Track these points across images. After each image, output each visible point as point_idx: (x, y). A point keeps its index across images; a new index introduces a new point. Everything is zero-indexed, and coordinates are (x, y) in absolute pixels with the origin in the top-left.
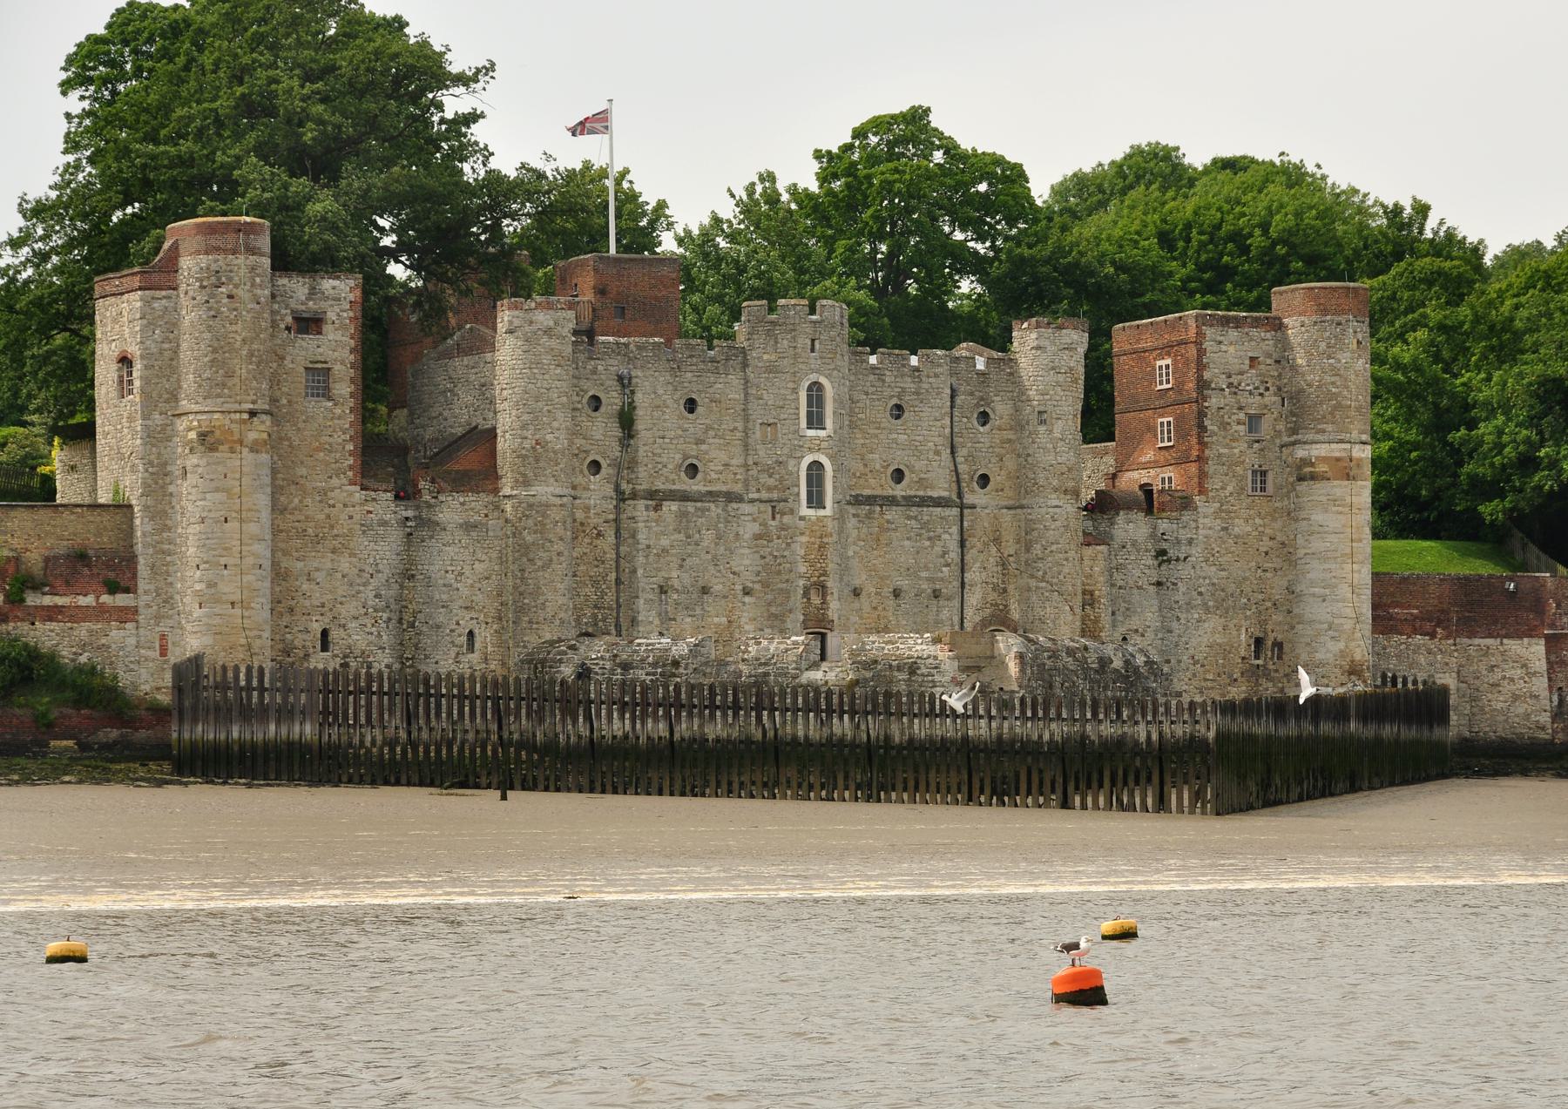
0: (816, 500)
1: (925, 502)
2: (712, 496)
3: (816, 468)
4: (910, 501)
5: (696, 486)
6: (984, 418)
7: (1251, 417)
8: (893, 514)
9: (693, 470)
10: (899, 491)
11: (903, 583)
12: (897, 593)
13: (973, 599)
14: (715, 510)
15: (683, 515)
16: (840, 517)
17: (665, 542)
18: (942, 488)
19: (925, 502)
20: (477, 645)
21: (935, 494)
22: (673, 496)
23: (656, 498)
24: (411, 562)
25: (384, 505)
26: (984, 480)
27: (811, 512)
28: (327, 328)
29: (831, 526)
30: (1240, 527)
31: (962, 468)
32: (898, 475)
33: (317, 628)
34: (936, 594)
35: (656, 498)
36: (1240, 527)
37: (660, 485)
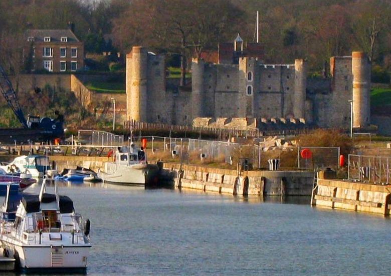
0: (249, 92)
1: (273, 92)
2: (231, 92)
3: (249, 88)
4: (271, 92)
5: (230, 90)
6: (288, 77)
7: (345, 76)
8: (268, 95)
9: (228, 88)
10: (270, 91)
11: (270, 107)
12: (268, 109)
13: (285, 110)
14: (232, 95)
15: (226, 95)
16: (255, 95)
17: (222, 100)
18: (278, 90)
19: (273, 92)
20: (187, 118)
21: (277, 91)
22: (223, 92)
23: (220, 92)
24: (175, 104)
25: (170, 94)
26: (288, 89)
27: (249, 95)
28: (160, 64)
29: (253, 98)
30: (342, 96)
31: (284, 86)
32: (269, 88)
33: (157, 115)
34: (276, 109)
35: (220, 92)
36: (342, 96)
37: (222, 90)
